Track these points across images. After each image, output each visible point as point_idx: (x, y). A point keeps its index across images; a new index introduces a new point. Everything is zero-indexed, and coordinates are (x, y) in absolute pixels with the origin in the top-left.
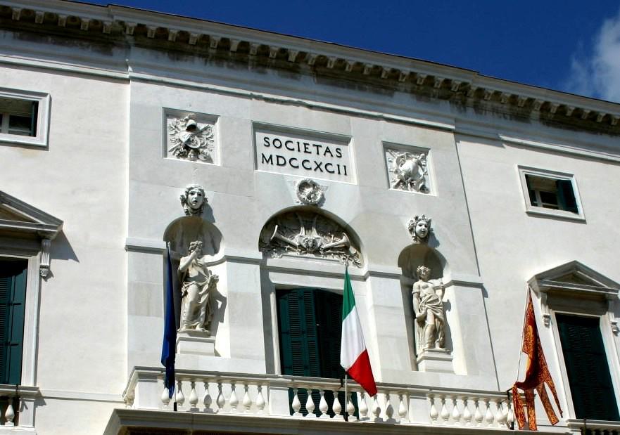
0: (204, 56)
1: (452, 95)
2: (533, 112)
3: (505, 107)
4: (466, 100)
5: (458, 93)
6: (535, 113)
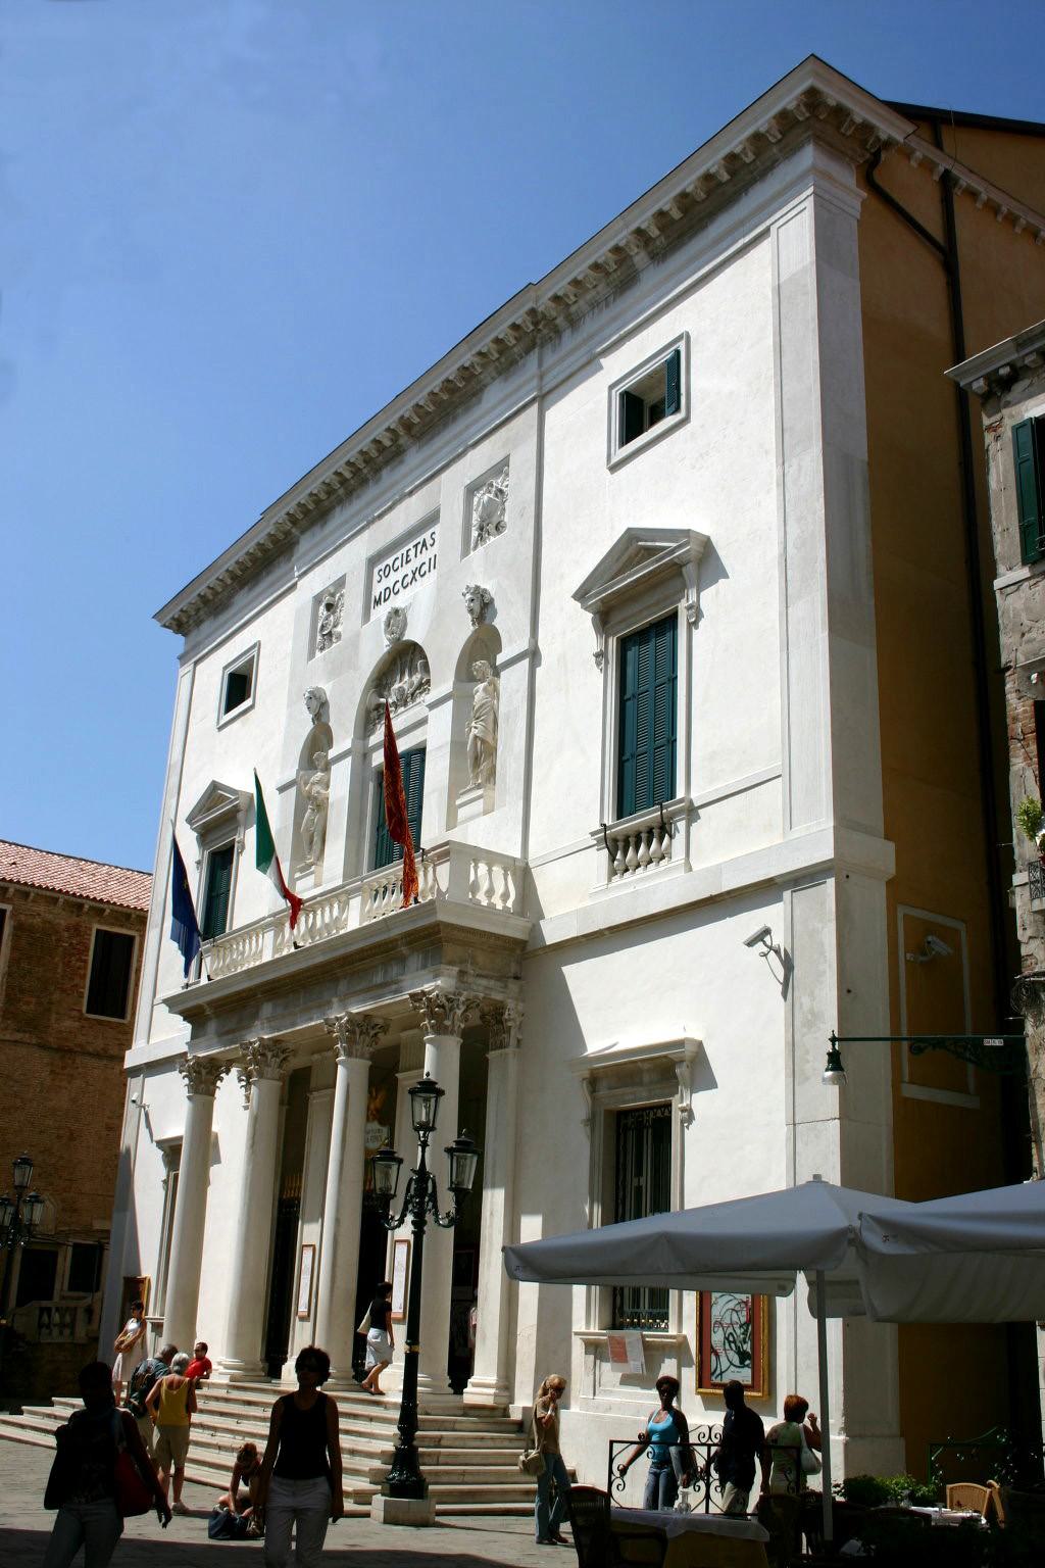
0: (340, 501)
1: (535, 338)
2: (636, 259)
3: (599, 288)
4: (556, 326)
5: (540, 327)
6: (640, 258)
